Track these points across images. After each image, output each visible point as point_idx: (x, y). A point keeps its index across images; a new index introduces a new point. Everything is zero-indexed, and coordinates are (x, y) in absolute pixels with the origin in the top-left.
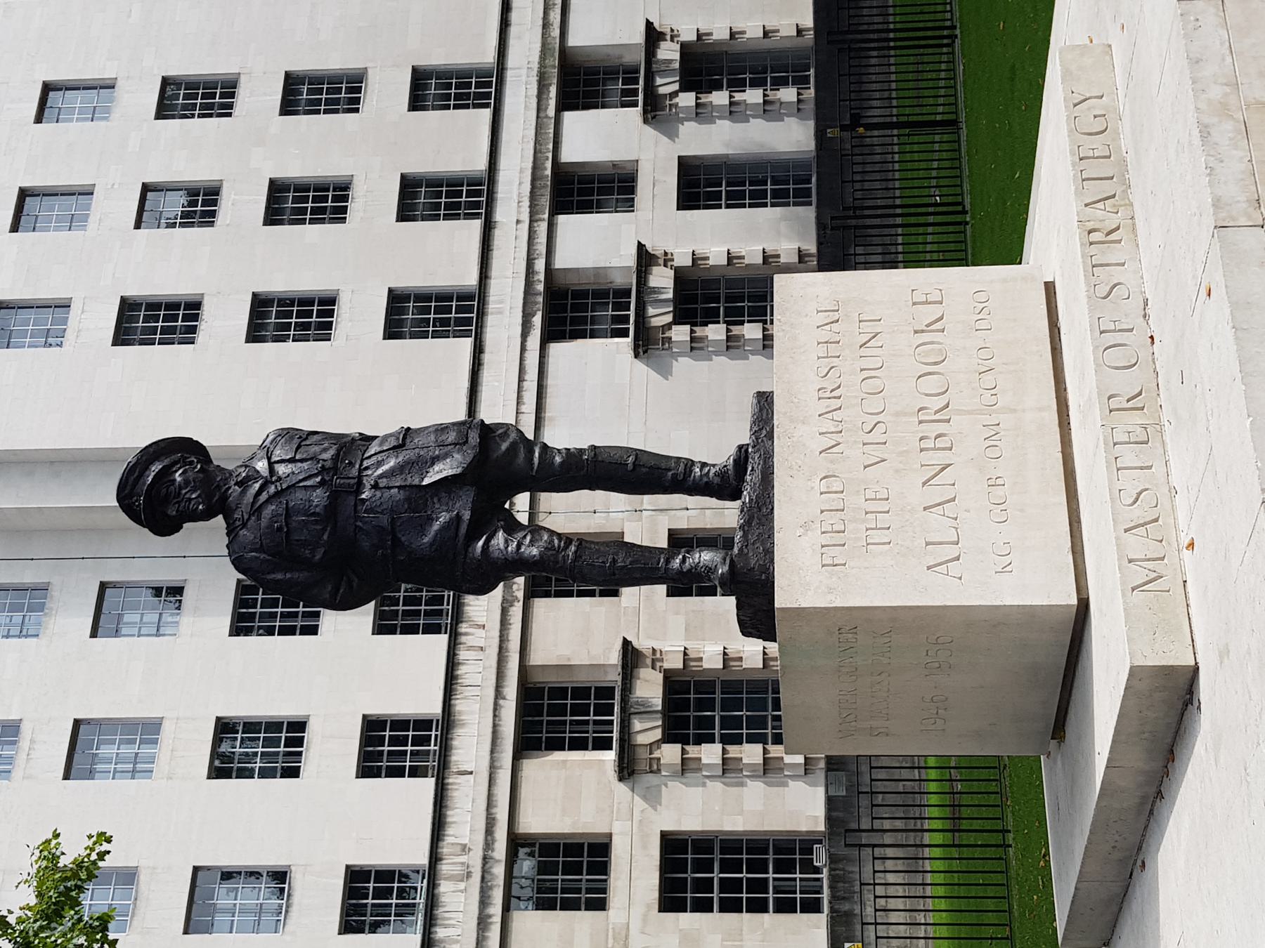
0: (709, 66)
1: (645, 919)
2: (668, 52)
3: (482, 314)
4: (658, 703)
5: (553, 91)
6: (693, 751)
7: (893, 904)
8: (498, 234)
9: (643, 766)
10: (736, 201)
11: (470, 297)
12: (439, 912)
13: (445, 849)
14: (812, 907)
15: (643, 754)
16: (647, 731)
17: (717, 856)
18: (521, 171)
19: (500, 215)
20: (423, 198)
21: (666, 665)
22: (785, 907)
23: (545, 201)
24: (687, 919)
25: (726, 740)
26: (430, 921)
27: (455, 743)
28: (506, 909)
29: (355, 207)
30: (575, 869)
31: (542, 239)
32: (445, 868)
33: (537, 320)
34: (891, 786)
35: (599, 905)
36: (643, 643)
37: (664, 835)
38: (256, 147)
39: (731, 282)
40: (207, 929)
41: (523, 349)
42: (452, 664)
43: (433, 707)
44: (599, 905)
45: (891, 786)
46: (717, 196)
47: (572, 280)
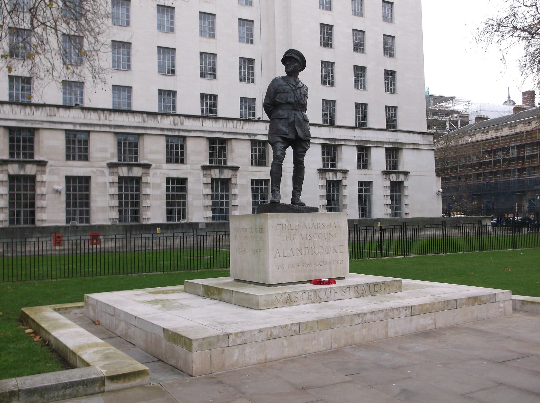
0: (397, 188)
1: (164, 174)
2: (402, 178)
3: (329, 126)
4: (223, 177)
5: (391, 146)
6: (210, 186)
7: (172, 241)
8: (350, 131)
9: (205, 172)
10: (360, 197)
11: (334, 123)
12: (165, 116)
13: (182, 118)
14: (168, 219)
15: (209, 172)
16: (215, 173)
17: (181, 193)
18: (369, 137)
19: (357, 131)
20: (361, 109)
21: (233, 179)
22: (168, 212)
23: (361, 144)
24: (164, 185)
25: (212, 195)
26: (163, 115)
27: (211, 121)
28: (166, 136)
29: (358, 91)
30: (177, 154)
31: (350, 143)
32: (177, 118)
33: (328, 142)
34: (202, 240)
35: (168, 161)
36: (239, 173)
37: (187, 179)
38: (375, 63)
39: (338, 196)
40: (159, 52)
41: (319, 138)
42: (232, 119)
43: (219, 115)
44: (168, 161)
45: (202, 240)
46: (362, 192)
47: (338, 152)
